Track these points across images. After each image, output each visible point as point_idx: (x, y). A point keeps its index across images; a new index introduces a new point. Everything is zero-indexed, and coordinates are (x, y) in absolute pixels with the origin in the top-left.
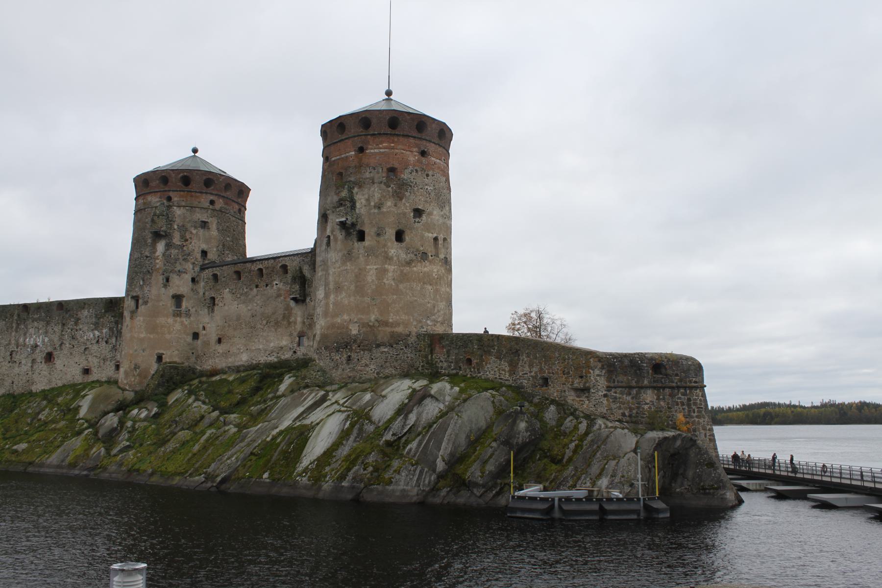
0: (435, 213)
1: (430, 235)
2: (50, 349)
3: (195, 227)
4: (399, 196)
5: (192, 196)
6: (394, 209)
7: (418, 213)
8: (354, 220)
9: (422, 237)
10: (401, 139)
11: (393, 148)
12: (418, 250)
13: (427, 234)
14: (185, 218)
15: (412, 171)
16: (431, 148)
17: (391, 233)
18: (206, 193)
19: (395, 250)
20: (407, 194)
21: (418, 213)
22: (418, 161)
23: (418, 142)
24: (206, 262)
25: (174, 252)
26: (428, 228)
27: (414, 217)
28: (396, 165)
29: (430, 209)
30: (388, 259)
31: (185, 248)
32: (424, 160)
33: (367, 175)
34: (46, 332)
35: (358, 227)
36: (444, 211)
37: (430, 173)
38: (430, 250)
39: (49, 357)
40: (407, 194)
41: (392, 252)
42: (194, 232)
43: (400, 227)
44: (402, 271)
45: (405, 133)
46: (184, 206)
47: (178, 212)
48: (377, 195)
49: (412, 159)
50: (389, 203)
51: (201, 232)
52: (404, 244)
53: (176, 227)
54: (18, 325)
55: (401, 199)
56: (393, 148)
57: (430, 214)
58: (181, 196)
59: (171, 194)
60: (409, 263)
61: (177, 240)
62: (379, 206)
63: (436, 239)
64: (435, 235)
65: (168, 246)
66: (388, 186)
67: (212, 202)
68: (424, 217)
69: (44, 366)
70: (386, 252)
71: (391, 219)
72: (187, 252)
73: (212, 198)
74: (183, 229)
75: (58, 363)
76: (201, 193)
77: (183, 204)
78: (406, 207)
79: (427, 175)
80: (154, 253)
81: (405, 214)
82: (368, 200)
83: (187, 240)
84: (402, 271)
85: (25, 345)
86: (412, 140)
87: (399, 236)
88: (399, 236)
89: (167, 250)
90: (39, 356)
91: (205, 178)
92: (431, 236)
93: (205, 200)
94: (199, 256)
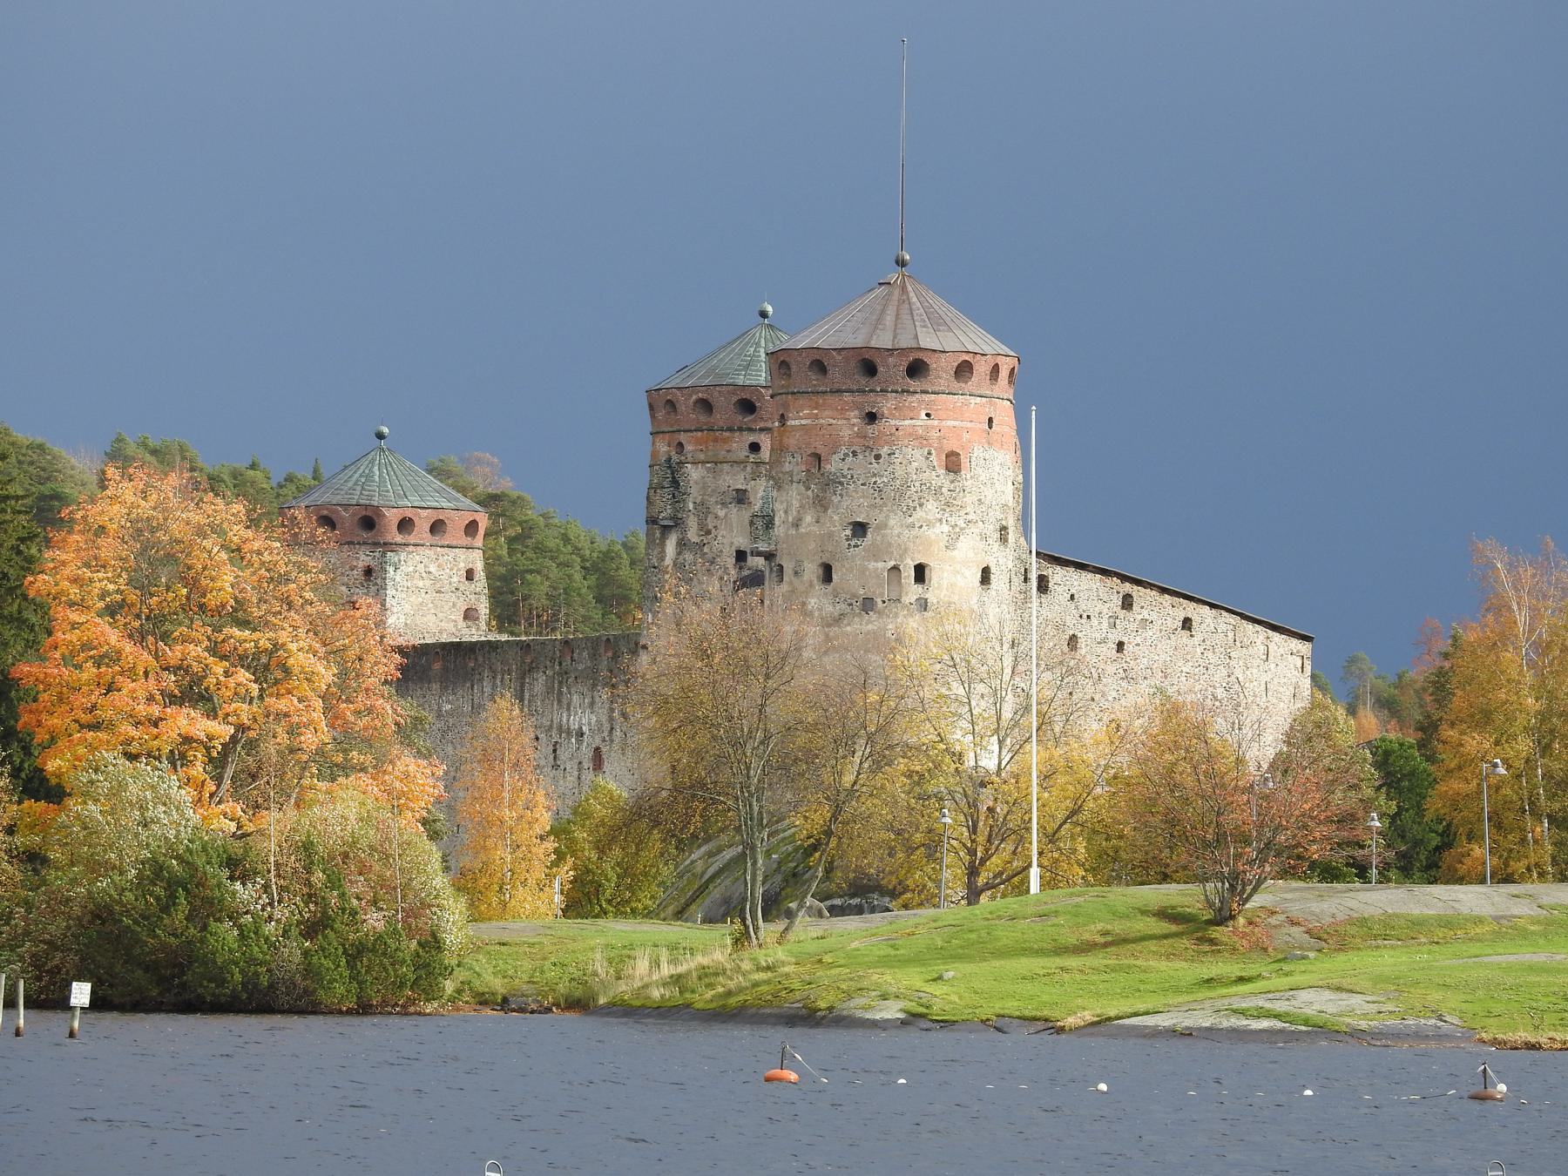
0: (892, 522)
1: (880, 565)
2: (597, 742)
3: (724, 504)
4: (821, 504)
5: (716, 440)
6: (815, 529)
7: (860, 529)
8: (773, 547)
9: (864, 570)
10: (828, 397)
11: (816, 417)
12: (854, 596)
13: (872, 565)
14: (704, 488)
15: (846, 455)
16: (887, 405)
17: (811, 571)
18: (740, 429)
19: (819, 601)
20: (836, 499)
21: (860, 529)
22: (858, 435)
23: (859, 398)
24: (746, 573)
25: (689, 556)
26: (876, 554)
27: (854, 535)
28: (821, 450)
29: (881, 517)
30: (806, 613)
31: (706, 550)
32: (870, 429)
33: (787, 467)
34: (592, 704)
35: (778, 560)
36: (919, 514)
37: (885, 451)
38: (881, 593)
39: (598, 760)
40: (836, 499)
41: (812, 602)
42: (721, 513)
43: (825, 560)
44: (827, 635)
45: (836, 386)
46: (703, 463)
47: (694, 473)
48: (796, 504)
49: (846, 433)
50: (808, 519)
51: (734, 509)
52: (830, 588)
53: (691, 506)
54: (560, 683)
55: (826, 509)
56: (816, 417)
57: (883, 526)
58: (698, 441)
59: (683, 437)
60: (838, 620)
61: (693, 535)
62: (796, 525)
63: (896, 568)
64: (892, 563)
65: (682, 545)
66: (808, 488)
67: (755, 447)
68: (869, 535)
69: (588, 776)
70: (804, 604)
71: (812, 546)
72: (710, 556)
73: (752, 438)
74: (703, 509)
75: (606, 766)
76: (730, 430)
77: (702, 457)
78: (836, 524)
79: (878, 457)
80: (663, 560)
81: (830, 535)
82: (786, 512)
83: (708, 532)
84: (827, 635)
85: (569, 733)
86: (847, 397)
87: (827, 573)
88: (827, 573)
89: (679, 554)
90: (586, 753)
91: (735, 399)
92: (882, 566)
93: (738, 445)
94: (731, 561)
